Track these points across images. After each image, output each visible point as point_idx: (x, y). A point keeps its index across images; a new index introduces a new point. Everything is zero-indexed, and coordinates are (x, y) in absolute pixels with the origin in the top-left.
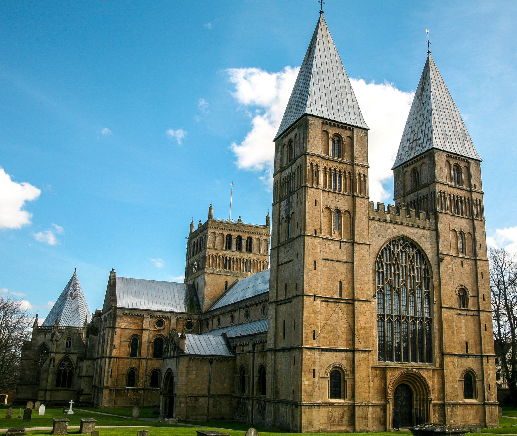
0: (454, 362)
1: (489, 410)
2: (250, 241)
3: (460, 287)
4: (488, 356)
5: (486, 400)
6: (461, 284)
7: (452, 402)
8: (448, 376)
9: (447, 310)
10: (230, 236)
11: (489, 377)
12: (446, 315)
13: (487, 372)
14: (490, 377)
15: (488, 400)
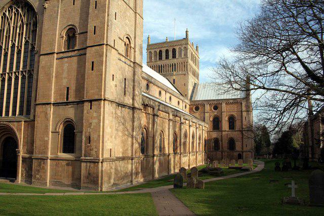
0: (46, 113)
1: (86, 168)
2: (174, 51)
3: (68, 28)
4: (91, 101)
5: (83, 155)
6: (70, 23)
7: (40, 156)
8: (38, 128)
9: (46, 56)
10: (161, 51)
11: (90, 127)
12: (44, 62)
13: (88, 121)
14: (92, 127)
15: (85, 156)
